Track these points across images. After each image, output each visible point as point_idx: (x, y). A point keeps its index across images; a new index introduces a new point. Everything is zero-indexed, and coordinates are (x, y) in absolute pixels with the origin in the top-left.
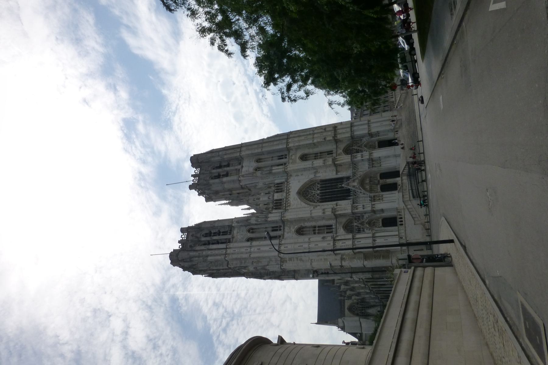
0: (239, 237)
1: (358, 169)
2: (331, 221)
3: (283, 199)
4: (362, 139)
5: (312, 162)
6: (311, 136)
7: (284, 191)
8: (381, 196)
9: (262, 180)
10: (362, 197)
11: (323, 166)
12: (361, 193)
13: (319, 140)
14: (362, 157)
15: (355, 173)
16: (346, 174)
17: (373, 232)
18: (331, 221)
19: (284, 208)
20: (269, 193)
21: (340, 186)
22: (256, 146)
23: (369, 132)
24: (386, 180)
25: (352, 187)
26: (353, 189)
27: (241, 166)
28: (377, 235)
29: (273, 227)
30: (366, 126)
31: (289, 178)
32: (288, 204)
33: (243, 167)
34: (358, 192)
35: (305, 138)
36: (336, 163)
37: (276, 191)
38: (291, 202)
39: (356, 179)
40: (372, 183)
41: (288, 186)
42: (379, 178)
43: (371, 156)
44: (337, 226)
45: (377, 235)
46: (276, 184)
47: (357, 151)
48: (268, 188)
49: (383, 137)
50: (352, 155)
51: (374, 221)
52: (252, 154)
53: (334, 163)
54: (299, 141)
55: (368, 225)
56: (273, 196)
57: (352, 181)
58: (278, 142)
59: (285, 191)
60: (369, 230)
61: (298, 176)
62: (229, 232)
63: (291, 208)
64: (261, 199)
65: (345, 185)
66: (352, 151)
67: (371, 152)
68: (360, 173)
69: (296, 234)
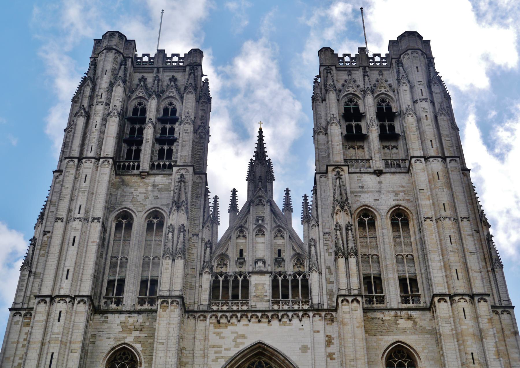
0: (142, 190)
7: (277, 303)
9: (324, 234)
19: (215, 308)
20: (279, 260)
31: (323, 314)
32: (227, 317)
37: (280, 279)
38: (230, 328)
41: (290, 314)
46: (304, 276)
48: (298, 254)
54: (458, 336)
56: (262, 273)
59: (276, 307)
61: (329, 342)
62: (162, 163)
64: (260, 239)
69: (112, 349)
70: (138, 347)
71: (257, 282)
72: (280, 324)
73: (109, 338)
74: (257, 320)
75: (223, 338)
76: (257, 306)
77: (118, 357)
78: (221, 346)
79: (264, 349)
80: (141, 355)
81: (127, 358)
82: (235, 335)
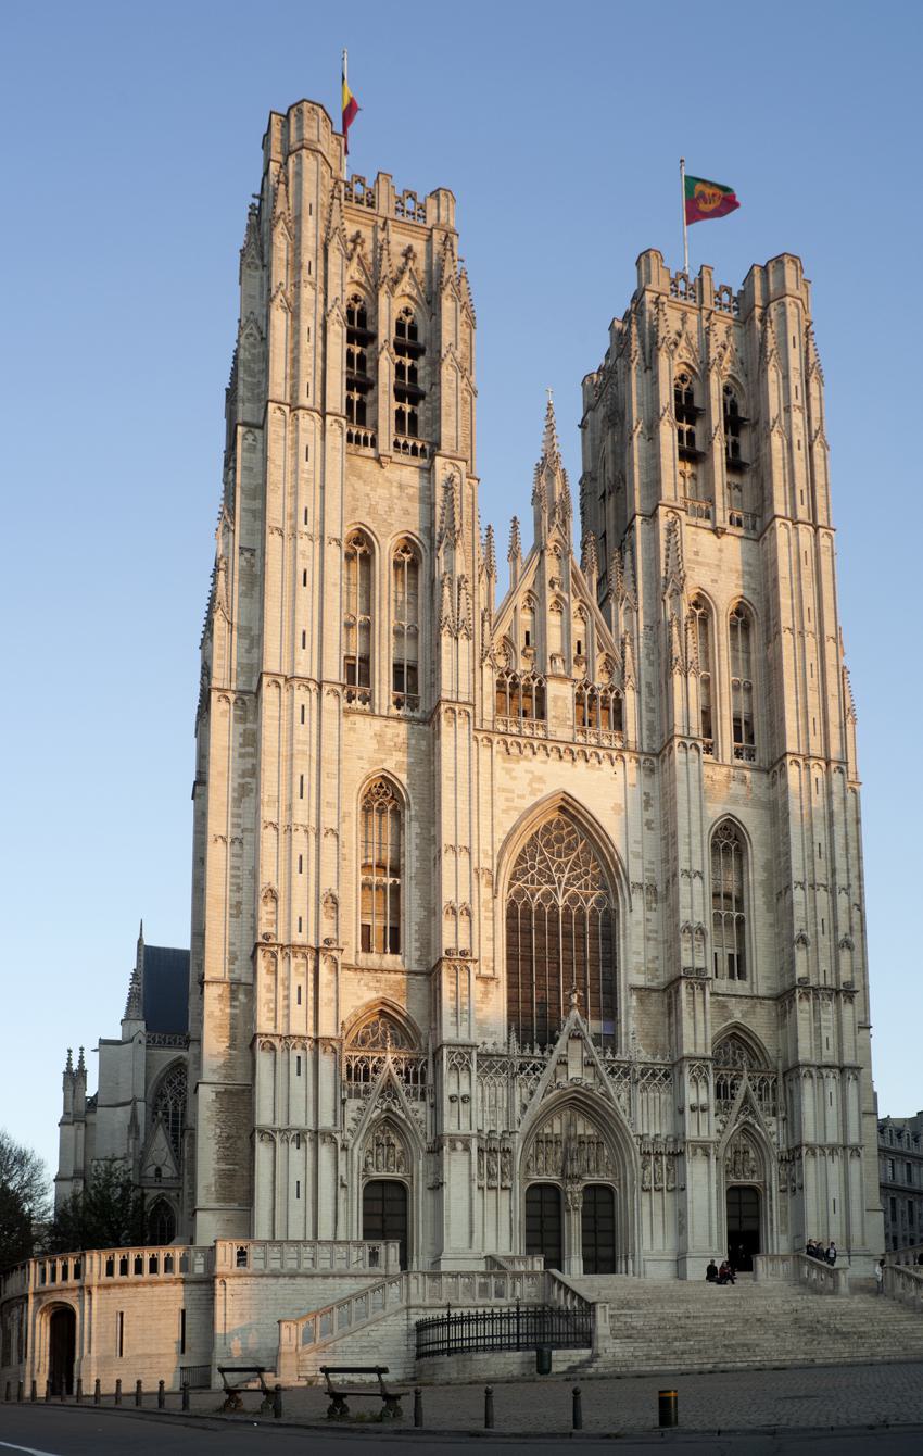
1: (644, 1088)
2: (417, 949)
3: (544, 727)
4: (781, 1115)
5: (700, 874)
6: (821, 878)
7: (584, 732)
8: (509, 1184)
10: (510, 1099)
11: (677, 925)
12: (532, 1093)
13: (799, 912)
14: (693, 1109)
15: (626, 1074)
16: (627, 1034)
17: (337, 1136)
18: (417, 949)
19: (501, 728)
21: (575, 999)
22: (809, 601)
23: (804, 1150)
24: (576, 1209)
25: (564, 1052)
26: (555, 1057)
27: (727, 525)
28: (325, 1152)
29: (413, 669)
30: (833, 1137)
32: (519, 744)
33: (719, 538)
34: (538, 1079)
35: (816, 848)
36: (683, 985)
38: (524, 763)
39: (597, 1074)
40: (574, 1145)
41: (601, 752)
42: (592, 1179)
43: (695, 1154)
44: (389, 971)
45: (325, 1152)
47: (725, 1086)
49: (775, 1207)
50: (710, 1065)
51: (398, 1147)
52: (776, 580)
53: (681, 977)
55: (379, 1115)
57: (591, 1056)
58: (815, 712)
59: (580, 738)
60: (354, 1120)
63: (498, 759)
65: (577, 1023)
66: (730, 1066)
67: (712, 1151)
68: (624, 1096)
70: (403, 778)
71: (558, 694)
72: (587, 768)
73: (361, 758)
74: (558, 756)
75: (514, 778)
76: (558, 734)
77: (374, 790)
78: (512, 791)
79: (567, 802)
80: (409, 792)
81: (385, 794)
82: (530, 776)
